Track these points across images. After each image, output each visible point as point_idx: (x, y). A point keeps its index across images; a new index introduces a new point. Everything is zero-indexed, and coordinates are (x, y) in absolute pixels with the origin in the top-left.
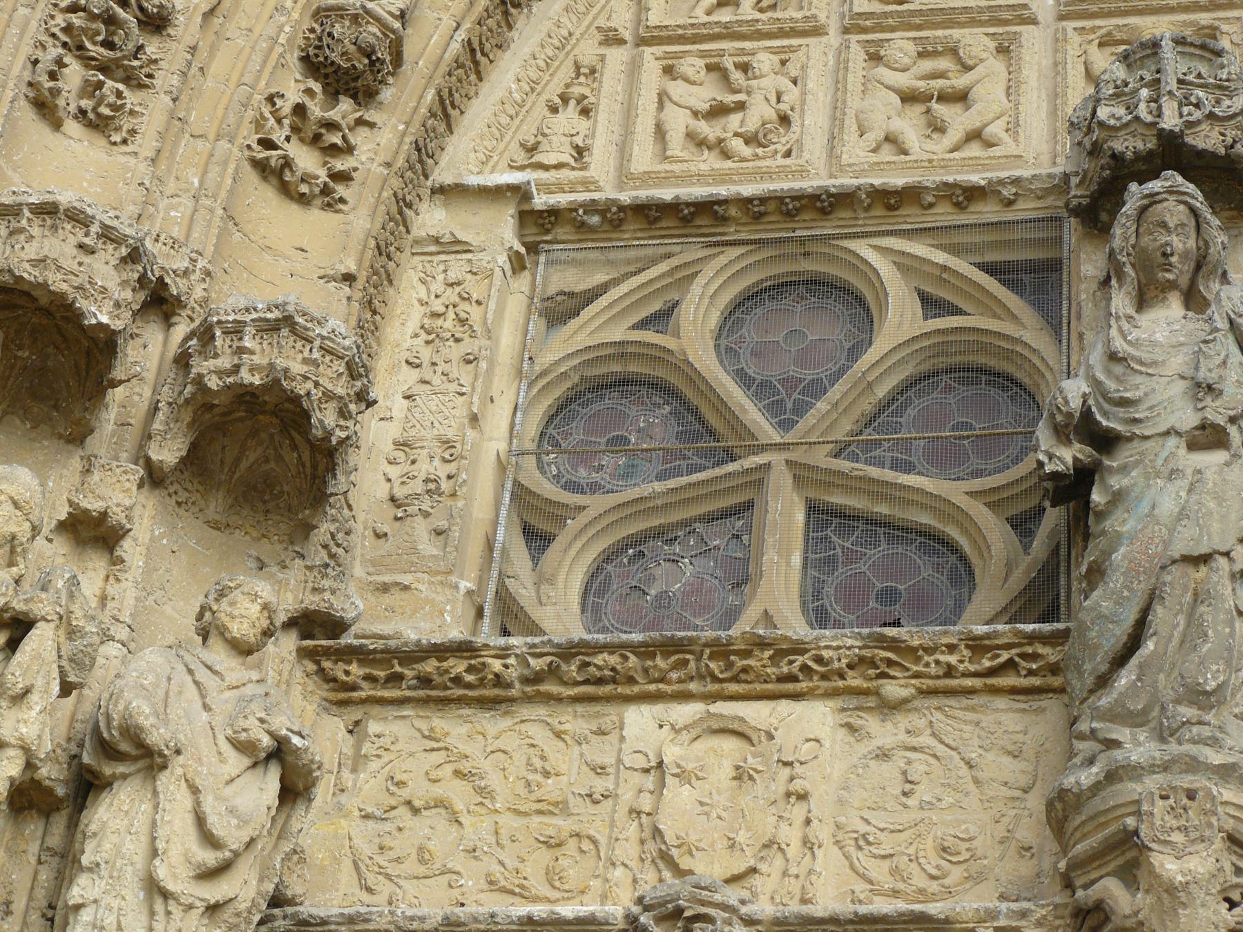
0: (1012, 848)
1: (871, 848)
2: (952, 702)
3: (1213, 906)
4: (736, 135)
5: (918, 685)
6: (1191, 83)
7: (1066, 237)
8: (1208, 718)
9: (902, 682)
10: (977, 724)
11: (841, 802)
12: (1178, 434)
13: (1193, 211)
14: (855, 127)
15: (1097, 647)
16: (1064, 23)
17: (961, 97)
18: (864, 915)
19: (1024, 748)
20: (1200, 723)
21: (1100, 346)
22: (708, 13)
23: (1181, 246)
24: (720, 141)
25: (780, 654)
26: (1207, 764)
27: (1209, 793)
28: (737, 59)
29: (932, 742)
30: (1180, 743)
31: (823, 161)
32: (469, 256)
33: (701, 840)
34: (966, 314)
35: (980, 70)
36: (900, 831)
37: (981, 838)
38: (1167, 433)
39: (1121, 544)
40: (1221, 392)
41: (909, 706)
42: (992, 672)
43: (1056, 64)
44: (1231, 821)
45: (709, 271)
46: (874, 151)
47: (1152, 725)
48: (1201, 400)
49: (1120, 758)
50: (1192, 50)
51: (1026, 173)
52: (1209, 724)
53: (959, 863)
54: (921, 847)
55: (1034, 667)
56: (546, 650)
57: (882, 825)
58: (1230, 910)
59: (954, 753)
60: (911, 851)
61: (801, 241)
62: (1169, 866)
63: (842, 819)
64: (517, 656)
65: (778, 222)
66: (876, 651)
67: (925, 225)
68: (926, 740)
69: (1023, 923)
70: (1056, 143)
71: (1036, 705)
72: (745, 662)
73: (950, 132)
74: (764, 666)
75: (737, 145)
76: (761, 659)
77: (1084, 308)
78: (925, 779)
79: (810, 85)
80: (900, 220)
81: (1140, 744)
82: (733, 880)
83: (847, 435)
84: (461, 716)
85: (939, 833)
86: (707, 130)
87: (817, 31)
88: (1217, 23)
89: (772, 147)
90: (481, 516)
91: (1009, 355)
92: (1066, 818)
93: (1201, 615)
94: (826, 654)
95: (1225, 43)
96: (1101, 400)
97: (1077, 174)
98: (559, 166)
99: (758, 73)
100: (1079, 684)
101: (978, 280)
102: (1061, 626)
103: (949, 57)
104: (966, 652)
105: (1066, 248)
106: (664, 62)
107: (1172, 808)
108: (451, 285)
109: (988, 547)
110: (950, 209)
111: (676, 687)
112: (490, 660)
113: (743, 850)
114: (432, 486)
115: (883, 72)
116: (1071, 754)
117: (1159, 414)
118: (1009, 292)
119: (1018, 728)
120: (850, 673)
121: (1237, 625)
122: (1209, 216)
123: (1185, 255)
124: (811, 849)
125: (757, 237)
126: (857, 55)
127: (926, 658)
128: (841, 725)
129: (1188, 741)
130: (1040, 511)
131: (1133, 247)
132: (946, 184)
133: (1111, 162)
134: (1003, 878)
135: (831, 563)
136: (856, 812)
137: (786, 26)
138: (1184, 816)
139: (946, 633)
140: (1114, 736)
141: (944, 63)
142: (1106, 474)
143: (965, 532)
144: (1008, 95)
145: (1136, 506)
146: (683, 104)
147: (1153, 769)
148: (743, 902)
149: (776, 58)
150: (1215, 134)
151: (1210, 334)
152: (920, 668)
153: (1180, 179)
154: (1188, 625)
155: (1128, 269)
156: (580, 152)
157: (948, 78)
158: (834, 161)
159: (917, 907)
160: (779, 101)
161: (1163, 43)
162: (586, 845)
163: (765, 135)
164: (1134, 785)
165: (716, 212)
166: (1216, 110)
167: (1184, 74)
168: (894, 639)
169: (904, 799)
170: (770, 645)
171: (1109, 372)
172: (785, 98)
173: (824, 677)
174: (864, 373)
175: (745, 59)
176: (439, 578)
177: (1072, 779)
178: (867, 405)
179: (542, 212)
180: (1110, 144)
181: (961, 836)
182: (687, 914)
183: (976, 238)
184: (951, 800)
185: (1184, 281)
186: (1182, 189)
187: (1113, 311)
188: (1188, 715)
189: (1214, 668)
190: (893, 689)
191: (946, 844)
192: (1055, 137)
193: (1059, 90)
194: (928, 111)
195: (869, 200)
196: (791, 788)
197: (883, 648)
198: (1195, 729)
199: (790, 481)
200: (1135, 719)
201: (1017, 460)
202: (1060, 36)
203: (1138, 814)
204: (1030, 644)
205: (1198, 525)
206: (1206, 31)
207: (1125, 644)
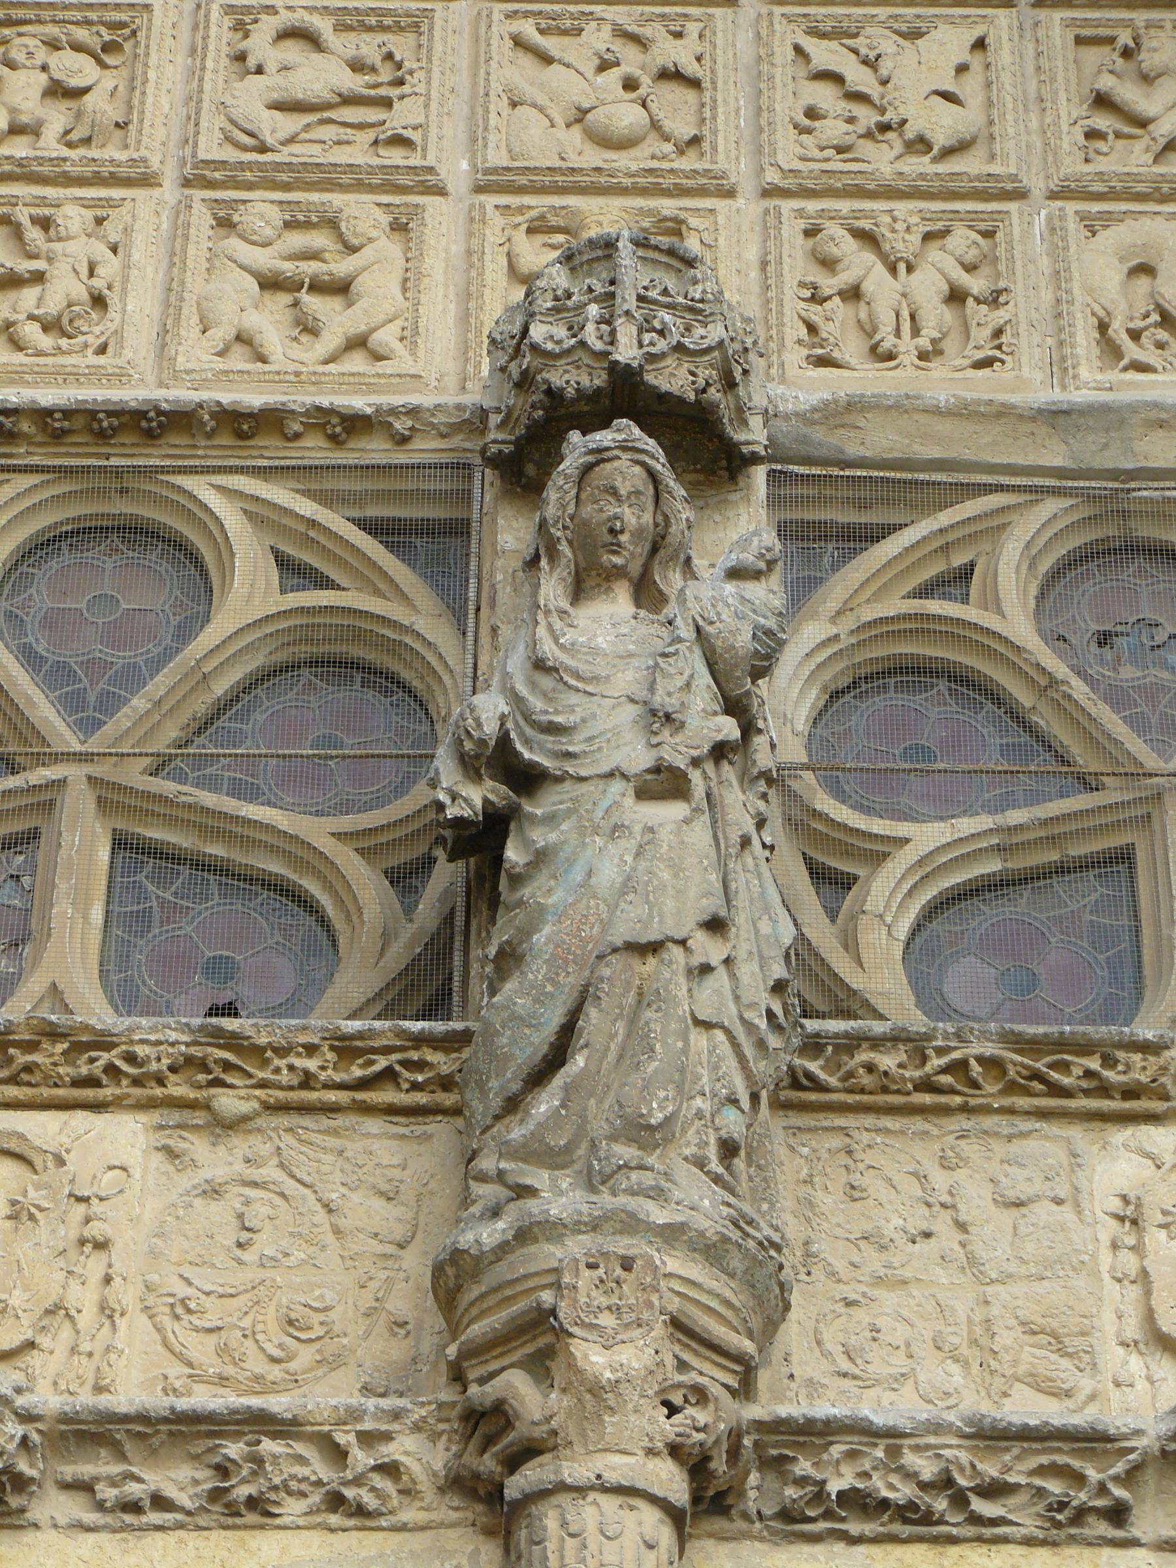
0: (381, 1322)
1: (193, 1318)
2: (307, 1121)
3: (650, 1412)
4: (32, 317)
5: (264, 1097)
6: (654, 302)
7: (477, 491)
8: (651, 1160)
9: (242, 1092)
10: (341, 1153)
11: (154, 1254)
12: (623, 776)
13: (652, 475)
14: (195, 319)
15: (507, 1058)
16: (483, 198)
17: (341, 288)
18: (183, 1412)
19: (402, 1187)
20: (641, 1167)
21: (521, 648)
23: (634, 521)
25: (78, 1048)
26: (648, 1223)
27: (650, 1261)
28: (35, 211)
29: (278, 1175)
30: (614, 1194)
31: (150, 362)
34: (339, 588)
35: (367, 253)
36: (232, 1296)
37: (339, 1309)
38: (610, 775)
39: (545, 922)
40: (682, 725)
41: (250, 1125)
42: (363, 1084)
43: (469, 253)
44: (677, 1299)
46: (220, 354)
47: (577, 1167)
48: (656, 734)
49: (535, 1211)
50: (656, 255)
51: (426, 400)
52: (651, 1169)
53: (311, 1341)
54: (260, 1318)
55: (420, 1079)
57: (208, 1287)
58: (668, 1417)
59: (307, 1191)
60: (246, 1323)
61: (118, 472)
62: (594, 1359)
63: (155, 1278)
65: (87, 444)
66: (209, 1049)
67: (288, 462)
68: (271, 1172)
69: (396, 1426)
70: (467, 360)
71: (419, 1129)
72: (29, 1058)
73: (325, 335)
74: (55, 1064)
75: (31, 332)
76: (52, 1055)
77: (500, 594)
78: (268, 1226)
79: (136, 256)
80: (255, 453)
81: (561, 1193)
83: (168, 747)
85: (284, 1300)
87: (147, 180)
88: (683, 215)
89: (81, 339)
91: (395, 648)
92: (459, 1288)
93: (647, 1023)
94: (141, 1051)
95: (692, 244)
96: (522, 722)
97: (498, 410)
99: (63, 234)
100: (480, 1107)
101: (358, 543)
102: (457, 1025)
103: (326, 231)
104: (331, 1056)
105: (476, 506)
107: (602, 1281)
109: (360, 910)
110: (323, 443)
113: (18, 1317)
115: (234, 244)
116: (466, 1201)
117: (600, 749)
118: (399, 563)
119: (395, 1161)
120: (173, 1078)
121: (692, 1037)
122: (672, 483)
123: (639, 533)
124: (111, 1317)
125: (57, 462)
126: (201, 219)
127: (277, 1062)
128: (157, 1149)
129: (624, 1191)
130: (428, 862)
131: (572, 518)
132: (319, 409)
133: (546, 399)
134: (368, 1363)
135: (143, 919)
136: (174, 1269)
137: (105, 170)
139: (305, 1028)
140: (528, 1181)
141: (319, 239)
142: (526, 825)
143: (328, 886)
144: (405, 290)
145: (566, 871)
147: (578, 1227)
148: (19, 1391)
149: (89, 214)
150: (683, 372)
151: (670, 645)
153: (637, 431)
154: (629, 1035)
155: (564, 547)
157: (324, 261)
158: (165, 364)
159: (255, 1402)
160: (91, 274)
161: (620, 244)
163: (71, 321)
164: (552, 1248)
166: (686, 341)
167: (645, 288)
168: (234, 1035)
169: (239, 1252)
170: (65, 1035)
171: (533, 685)
172: (99, 271)
173: (137, 1082)
174: (198, 661)
175: (47, 211)
177: (470, 1237)
178: (201, 705)
180: (545, 375)
181: (315, 1304)
183: (356, 486)
184: (303, 1256)
185: (635, 568)
186: (639, 445)
187: (542, 603)
188: (626, 1157)
189: (662, 1094)
190: (229, 1102)
191: (293, 1315)
192: (466, 353)
193: (473, 289)
194: (296, 304)
195: (213, 423)
196: (86, 1234)
197: (219, 1046)
198: (634, 1176)
199: (92, 805)
200: (555, 1159)
201: (400, 790)
202: (476, 214)
203: (557, 1286)
204: (416, 1048)
205: (648, 902)
206: (670, 224)
207: (546, 1056)
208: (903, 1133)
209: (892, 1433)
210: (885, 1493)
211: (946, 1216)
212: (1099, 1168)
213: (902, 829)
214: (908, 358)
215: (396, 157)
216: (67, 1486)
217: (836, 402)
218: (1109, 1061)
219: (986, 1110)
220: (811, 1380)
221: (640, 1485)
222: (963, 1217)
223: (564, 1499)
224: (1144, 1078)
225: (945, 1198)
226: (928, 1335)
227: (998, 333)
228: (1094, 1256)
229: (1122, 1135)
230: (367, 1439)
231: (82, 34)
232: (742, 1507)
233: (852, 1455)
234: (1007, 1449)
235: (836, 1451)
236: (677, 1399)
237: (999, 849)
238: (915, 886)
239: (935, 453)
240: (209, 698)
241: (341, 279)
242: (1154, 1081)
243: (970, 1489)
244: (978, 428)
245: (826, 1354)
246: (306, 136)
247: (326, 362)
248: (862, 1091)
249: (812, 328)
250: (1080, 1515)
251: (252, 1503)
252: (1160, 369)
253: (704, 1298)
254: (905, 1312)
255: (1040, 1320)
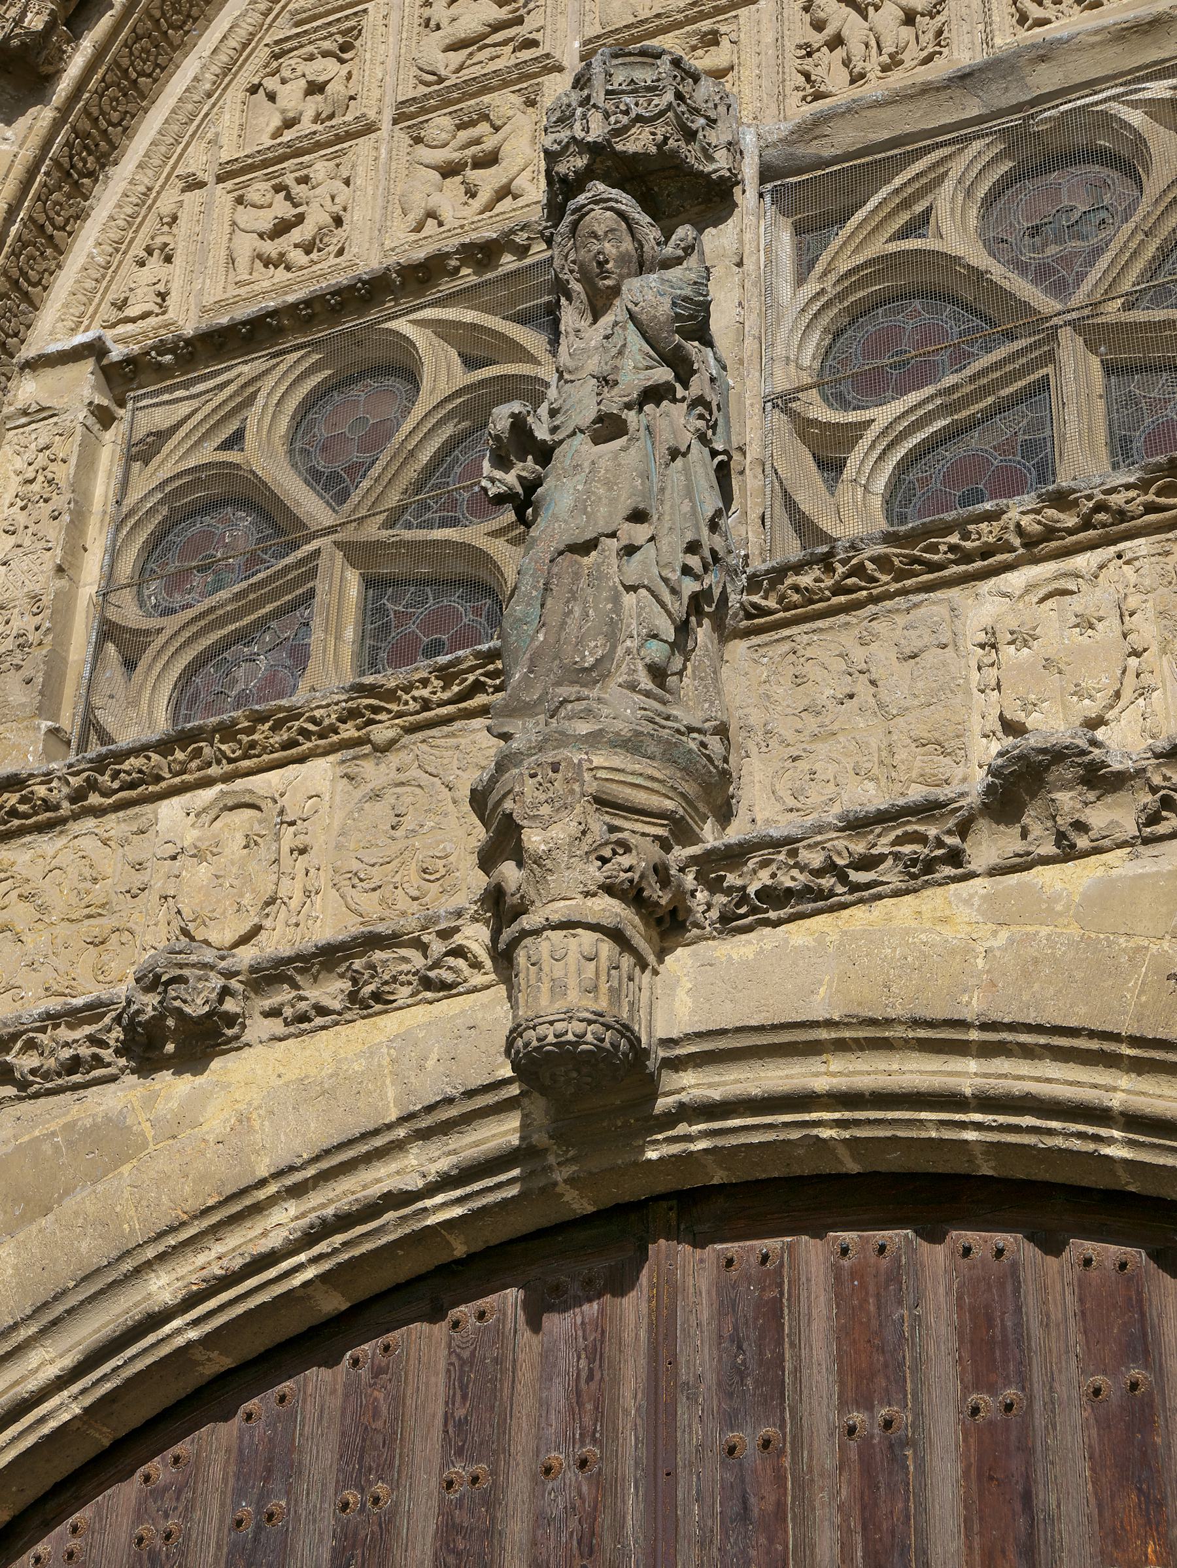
2: (434, 732)
5: (402, 724)
9: (387, 724)
11: (339, 847)
13: (621, 215)
22: (274, 136)
23: (614, 251)
24: (282, 255)
27: (569, 761)
28: (297, 174)
32: (55, 419)
33: (214, 911)
38: (574, 434)
41: (397, 746)
45: (269, 382)
50: (632, 59)
53: (438, 879)
56: (81, 767)
57: (372, 862)
60: (397, 878)
62: (534, 839)
64: (59, 778)
68: (415, 773)
82: (244, 940)
84: (24, 845)
86: (270, 248)
87: (370, 128)
88: (716, 27)
90: (76, 658)
94: (317, 713)
98: (145, 316)
104: (436, 683)
106: (236, 194)
107: (541, 784)
108: (41, 451)
111: (198, 775)
112: (36, 788)
114: (21, 640)
115: (423, 153)
120: (342, 726)
132: (463, 245)
136: (353, 854)
138: (552, 788)
140: (505, 730)
146: (249, 229)
152: (402, 708)
156: (163, 296)
162: (126, 937)
165: (270, 324)
173: (322, 736)
175: (305, 172)
176: (25, 723)
178: (411, 473)
179: (121, 362)
182: (164, 979)
184: (432, 824)
186: (604, 196)
189: (592, 644)
190: (382, 733)
208: (831, 628)
209: (789, 841)
210: (789, 883)
211: (864, 678)
212: (970, 615)
213: (866, 415)
214: (874, 73)
215: (526, 55)
216: (267, 1014)
217: (804, 122)
218: (966, 536)
219: (890, 596)
220: (767, 820)
221: (575, 918)
222: (874, 676)
223: (528, 941)
224: (991, 540)
225: (864, 666)
226: (850, 767)
227: (939, 33)
228: (966, 679)
229: (986, 586)
230: (444, 935)
231: (327, 45)
232: (691, 919)
233: (765, 864)
234: (872, 831)
235: (751, 864)
236: (607, 852)
237: (946, 409)
238: (884, 452)
239: (885, 135)
240: (418, 466)
241: (490, 152)
242: (1000, 539)
243: (847, 866)
244: (911, 107)
245: (779, 799)
246: (469, 62)
247: (482, 212)
248: (796, 607)
249: (807, 76)
250: (929, 866)
251: (377, 997)
252: (1054, 19)
253: (630, 779)
254: (834, 755)
255: (926, 735)
